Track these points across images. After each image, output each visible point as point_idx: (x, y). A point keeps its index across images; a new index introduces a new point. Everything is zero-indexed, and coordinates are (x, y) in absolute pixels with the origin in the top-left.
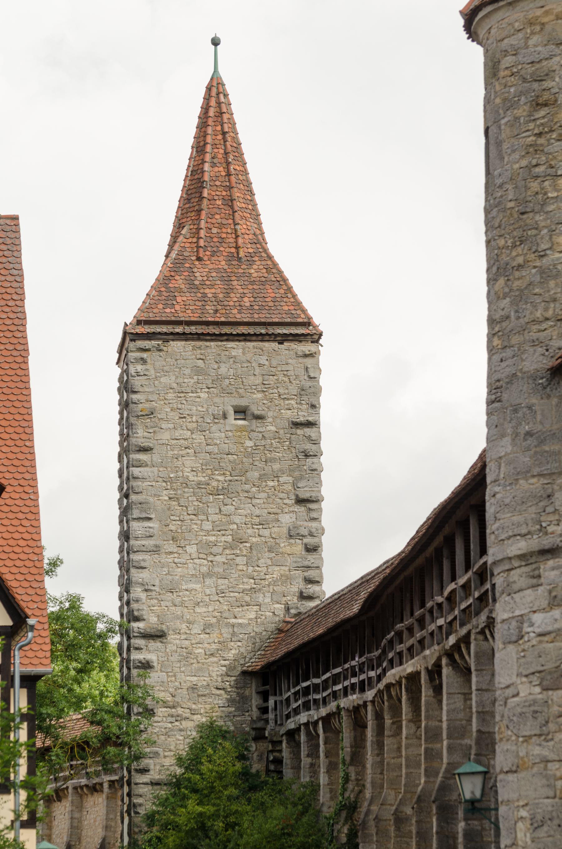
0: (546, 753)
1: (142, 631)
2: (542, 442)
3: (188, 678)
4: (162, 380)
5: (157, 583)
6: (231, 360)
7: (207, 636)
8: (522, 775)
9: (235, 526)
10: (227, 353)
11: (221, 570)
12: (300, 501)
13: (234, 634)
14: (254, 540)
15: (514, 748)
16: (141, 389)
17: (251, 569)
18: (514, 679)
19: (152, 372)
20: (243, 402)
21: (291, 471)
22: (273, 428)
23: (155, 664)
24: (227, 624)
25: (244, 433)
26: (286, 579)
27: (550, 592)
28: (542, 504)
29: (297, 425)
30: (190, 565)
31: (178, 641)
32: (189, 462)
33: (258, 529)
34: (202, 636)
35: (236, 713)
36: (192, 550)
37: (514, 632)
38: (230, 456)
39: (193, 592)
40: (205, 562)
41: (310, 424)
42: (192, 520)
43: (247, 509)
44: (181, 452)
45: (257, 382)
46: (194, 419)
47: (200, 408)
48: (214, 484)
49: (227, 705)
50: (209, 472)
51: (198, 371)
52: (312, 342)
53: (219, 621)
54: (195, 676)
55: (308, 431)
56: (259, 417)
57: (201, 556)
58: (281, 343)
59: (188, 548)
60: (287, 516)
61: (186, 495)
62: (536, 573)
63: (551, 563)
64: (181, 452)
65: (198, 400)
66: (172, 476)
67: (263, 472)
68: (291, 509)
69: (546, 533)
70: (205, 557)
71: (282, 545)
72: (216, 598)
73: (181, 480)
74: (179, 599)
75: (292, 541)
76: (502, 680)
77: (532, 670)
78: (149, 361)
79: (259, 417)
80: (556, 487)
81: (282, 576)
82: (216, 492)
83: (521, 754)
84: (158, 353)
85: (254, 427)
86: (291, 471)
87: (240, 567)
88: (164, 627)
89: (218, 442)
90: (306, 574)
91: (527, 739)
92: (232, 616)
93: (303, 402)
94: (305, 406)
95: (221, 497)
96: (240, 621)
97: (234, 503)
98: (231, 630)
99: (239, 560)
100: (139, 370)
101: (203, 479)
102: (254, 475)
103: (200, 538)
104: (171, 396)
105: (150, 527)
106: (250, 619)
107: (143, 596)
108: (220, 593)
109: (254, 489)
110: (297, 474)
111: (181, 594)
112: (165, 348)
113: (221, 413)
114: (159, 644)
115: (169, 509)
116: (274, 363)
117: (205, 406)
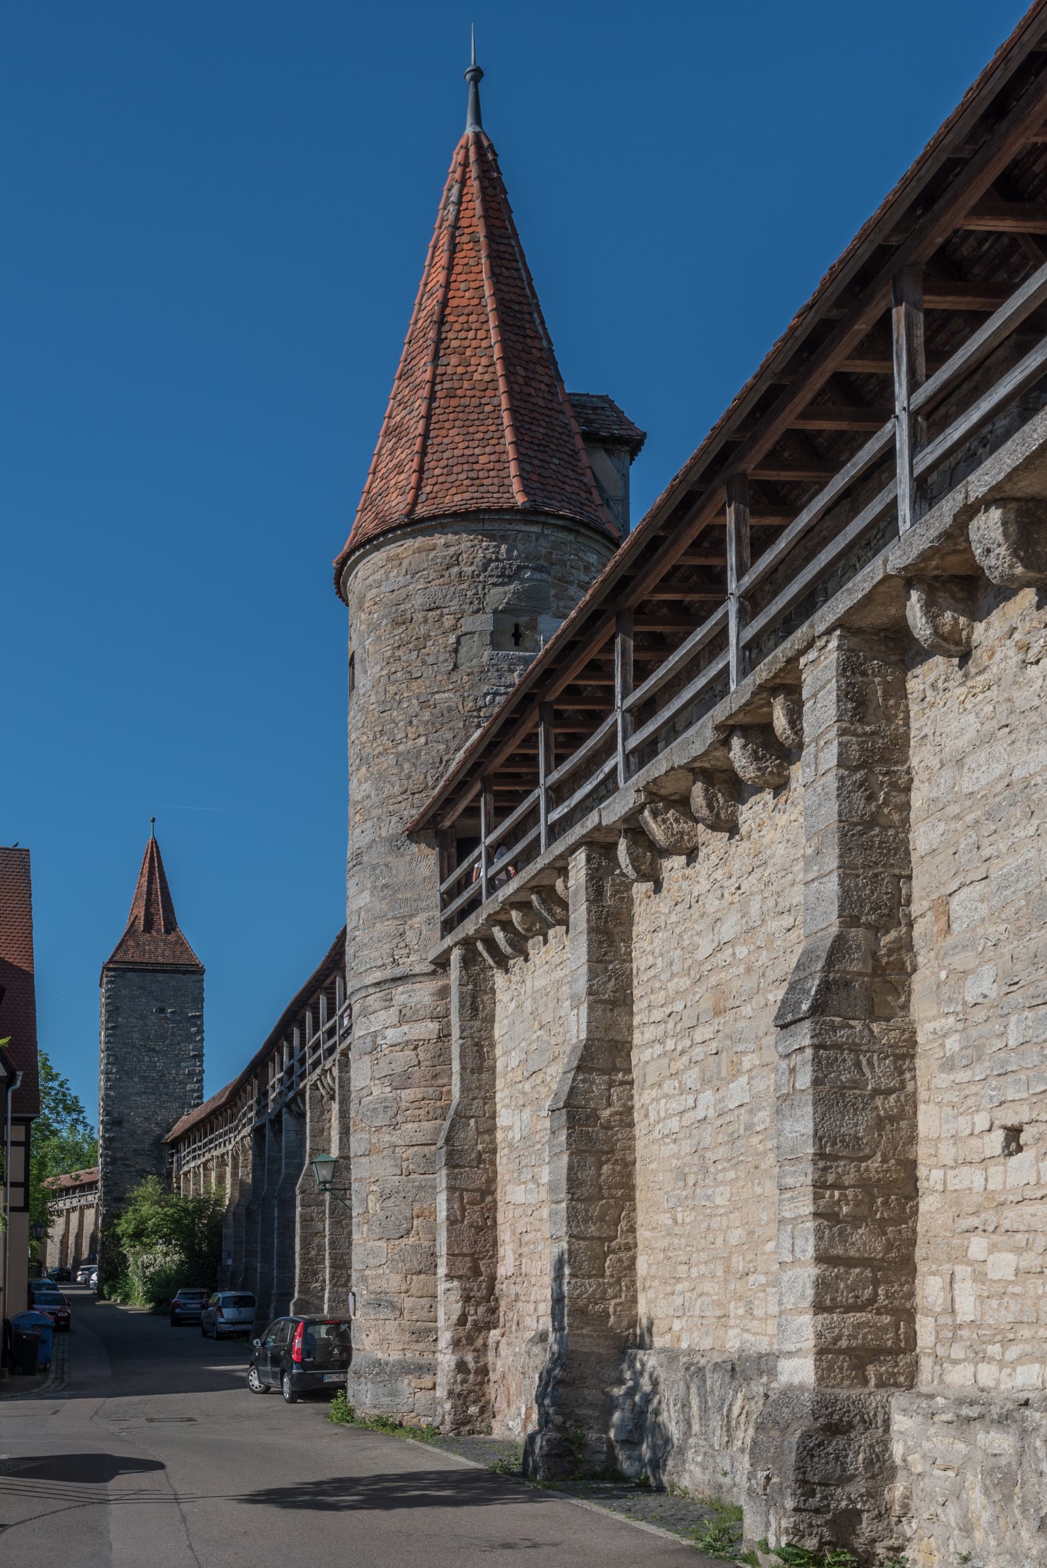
0: (394, 1139)
2: (395, 892)
8: (373, 1158)
15: (367, 1136)
18: (368, 1082)
27: (401, 1012)
28: (394, 941)
37: (369, 1046)
62: (389, 997)
63: (401, 989)
69: (398, 965)
76: (357, 1084)
77: (384, 1074)
80: (407, 927)
83: (373, 1141)
91: (379, 1129)
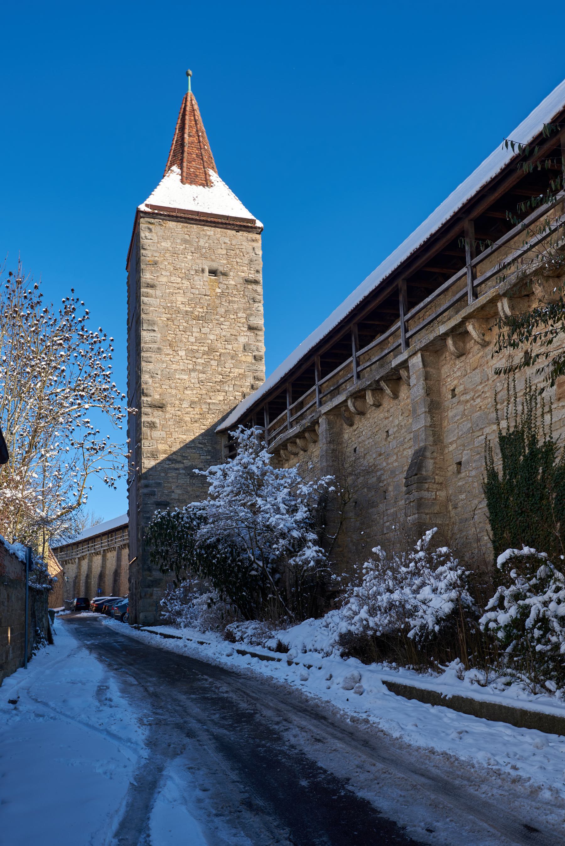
1: (149, 403)
3: (180, 436)
4: (162, 244)
5: (159, 373)
6: (207, 237)
7: (192, 409)
9: (210, 341)
10: (204, 233)
11: (201, 368)
12: (251, 328)
13: (209, 409)
14: (223, 351)
16: (148, 248)
17: (220, 369)
19: (155, 239)
20: (215, 266)
21: (245, 310)
22: (233, 283)
23: (158, 425)
24: (205, 402)
25: (215, 283)
26: (242, 376)
29: (248, 281)
30: (181, 363)
31: (173, 411)
32: (180, 299)
33: (225, 344)
34: (189, 409)
35: (212, 460)
36: (182, 353)
38: (206, 297)
39: (183, 381)
40: (191, 362)
41: (256, 282)
42: (182, 335)
43: (218, 331)
44: (175, 291)
45: (223, 253)
46: (183, 271)
47: (187, 265)
48: (197, 313)
49: (205, 454)
50: (193, 305)
51: (185, 241)
52: (257, 233)
53: (199, 400)
54: (184, 434)
55: (254, 287)
56: (225, 274)
57: (188, 358)
58: (238, 231)
59: (180, 352)
60: (243, 338)
61: (178, 318)
64: (175, 291)
65: (185, 259)
66: (169, 305)
67: (227, 309)
68: (245, 334)
70: (191, 359)
71: (240, 355)
72: (198, 385)
73: (175, 308)
74: (174, 385)
75: (246, 354)
78: (153, 230)
79: (225, 274)
81: (240, 374)
82: (197, 318)
84: (159, 227)
85: (221, 280)
86: (245, 310)
87: (213, 367)
88: (164, 402)
89: (199, 287)
90: (255, 375)
92: (208, 398)
93: (252, 269)
94: (252, 272)
95: (201, 322)
96: (214, 401)
97: (209, 326)
98: (208, 407)
99: (213, 362)
100: (147, 236)
101: (189, 309)
102: (222, 310)
103: (187, 347)
104: (167, 255)
105: (154, 336)
106: (220, 401)
107: (150, 381)
108: (200, 382)
109: (222, 319)
110: (248, 312)
111: (175, 381)
112: (164, 225)
113: (200, 269)
114: (161, 413)
115: (167, 326)
116: (234, 242)
117: (190, 264)
